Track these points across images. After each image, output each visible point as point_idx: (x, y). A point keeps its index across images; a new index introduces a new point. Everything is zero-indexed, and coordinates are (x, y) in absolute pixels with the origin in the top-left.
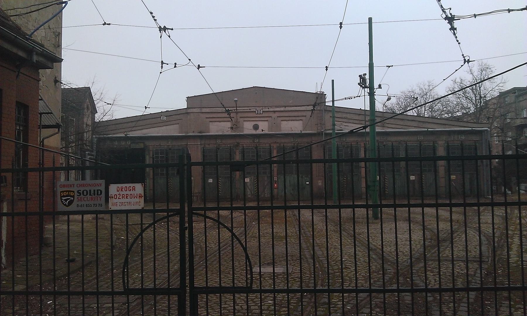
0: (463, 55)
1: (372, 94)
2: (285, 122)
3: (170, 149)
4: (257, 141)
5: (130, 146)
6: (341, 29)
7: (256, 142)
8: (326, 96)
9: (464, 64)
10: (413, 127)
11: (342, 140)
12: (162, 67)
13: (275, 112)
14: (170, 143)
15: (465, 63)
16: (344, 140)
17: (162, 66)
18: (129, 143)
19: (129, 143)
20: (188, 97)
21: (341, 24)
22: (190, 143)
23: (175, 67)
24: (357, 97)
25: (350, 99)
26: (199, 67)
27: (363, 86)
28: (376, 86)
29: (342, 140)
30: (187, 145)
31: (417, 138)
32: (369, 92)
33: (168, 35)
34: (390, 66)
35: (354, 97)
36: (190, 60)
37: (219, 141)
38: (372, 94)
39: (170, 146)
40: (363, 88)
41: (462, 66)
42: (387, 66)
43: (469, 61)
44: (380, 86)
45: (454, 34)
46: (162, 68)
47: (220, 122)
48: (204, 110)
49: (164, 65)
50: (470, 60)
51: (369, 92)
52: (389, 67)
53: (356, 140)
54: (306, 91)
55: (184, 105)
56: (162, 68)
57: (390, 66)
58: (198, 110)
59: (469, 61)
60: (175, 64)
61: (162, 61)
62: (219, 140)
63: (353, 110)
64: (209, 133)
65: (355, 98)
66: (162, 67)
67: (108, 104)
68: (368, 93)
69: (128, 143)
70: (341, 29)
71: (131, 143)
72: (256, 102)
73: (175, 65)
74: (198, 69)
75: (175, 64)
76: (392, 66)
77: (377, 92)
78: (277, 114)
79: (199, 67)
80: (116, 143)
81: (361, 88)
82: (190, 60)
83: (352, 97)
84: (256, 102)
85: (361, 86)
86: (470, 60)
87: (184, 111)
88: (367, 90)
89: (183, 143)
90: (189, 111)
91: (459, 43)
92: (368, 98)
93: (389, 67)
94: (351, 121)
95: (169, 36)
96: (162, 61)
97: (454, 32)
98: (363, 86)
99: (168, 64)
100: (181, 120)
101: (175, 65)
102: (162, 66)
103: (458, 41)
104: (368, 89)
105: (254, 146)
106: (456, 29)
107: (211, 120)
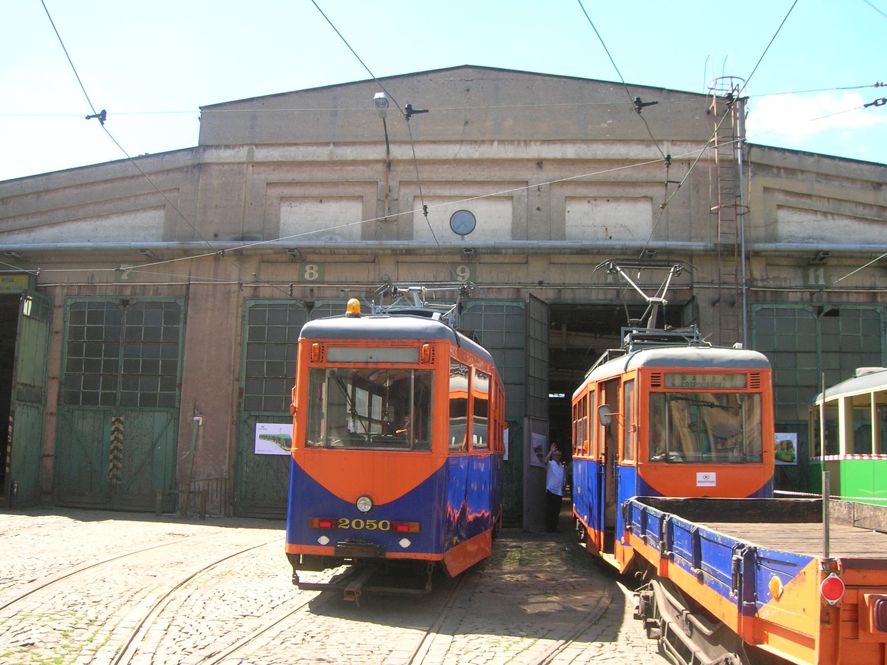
2: (583, 207)
3: (125, 303)
11: (812, 282)
13: (540, 163)
16: (821, 282)
29: (812, 282)
39: (128, 292)
54: (668, 87)
58: (242, 154)
62: (311, 268)
63: (854, 166)
72: (466, 123)
84: (466, 123)
87: (188, 160)
90: (211, 156)
94: (847, 209)
107: (287, 191)
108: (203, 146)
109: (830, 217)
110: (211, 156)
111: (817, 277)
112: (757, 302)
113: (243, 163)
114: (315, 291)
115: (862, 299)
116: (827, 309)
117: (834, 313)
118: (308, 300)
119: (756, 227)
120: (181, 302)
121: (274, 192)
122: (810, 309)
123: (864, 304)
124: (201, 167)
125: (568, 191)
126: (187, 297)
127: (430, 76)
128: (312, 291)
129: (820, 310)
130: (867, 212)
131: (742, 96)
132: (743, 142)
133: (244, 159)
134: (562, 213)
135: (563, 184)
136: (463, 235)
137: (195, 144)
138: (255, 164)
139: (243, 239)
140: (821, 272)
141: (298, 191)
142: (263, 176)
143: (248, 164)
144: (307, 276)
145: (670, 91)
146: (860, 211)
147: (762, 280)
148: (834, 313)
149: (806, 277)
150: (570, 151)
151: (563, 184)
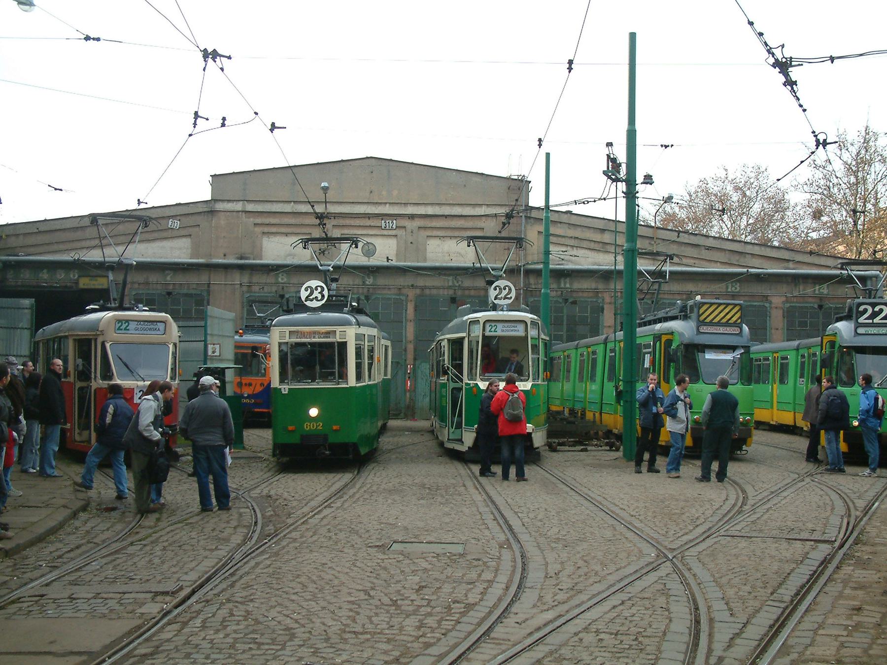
0: (813, 132)
1: (631, 196)
3: (169, 294)
4: (369, 281)
5: (77, 283)
6: (570, 72)
7: (367, 283)
8: (530, 185)
9: (817, 148)
10: (719, 264)
11: (562, 285)
12: (195, 124)
13: (412, 217)
14: (168, 278)
15: (817, 146)
16: (568, 286)
17: (195, 121)
18: (74, 276)
19: (74, 276)
20: (215, 175)
21: (571, 62)
22: (218, 279)
23: (223, 125)
24: (600, 199)
25: (584, 203)
26: (273, 127)
27: (613, 177)
28: (639, 178)
29: (562, 285)
30: (209, 285)
31: (727, 288)
32: (625, 191)
33: (221, 66)
34: (668, 146)
35: (593, 200)
36: (256, 113)
37: (282, 279)
38: (631, 196)
39: (171, 287)
40: (614, 181)
41: (813, 153)
42: (662, 146)
43: (825, 144)
44: (648, 180)
45: (793, 91)
46: (195, 127)
47: (287, 234)
48: (250, 207)
49: (199, 120)
50: (828, 141)
51: (625, 191)
52: (666, 147)
53: (593, 286)
55: (205, 193)
56: (195, 127)
57: (668, 146)
58: (238, 206)
59: (825, 144)
60: (224, 119)
61: (196, 113)
63: (590, 220)
64: (261, 260)
65: (595, 201)
66: (195, 124)
67: (56, 189)
68: (623, 192)
69: (72, 276)
70: (570, 72)
71: (79, 276)
73: (224, 122)
74: (272, 130)
75: (224, 119)
76: (672, 146)
77: (642, 190)
78: (418, 223)
79: (273, 127)
80: (45, 275)
81: (609, 181)
82: (256, 113)
83: (589, 200)
85: (609, 177)
86: (828, 141)
88: (622, 186)
89: (204, 278)
90: (220, 206)
91: (804, 110)
92: (622, 203)
93: (666, 147)
95: (222, 69)
96: (196, 113)
97: (792, 88)
98: (613, 177)
99: (207, 119)
100: (197, 229)
101: (224, 122)
102: (195, 121)
103: (801, 106)
104: (624, 183)
105: (363, 294)
106: (795, 83)
107: (266, 230)
108: (214, 200)
109: (575, 249)
110: (220, 206)
111: (566, 284)
112: (532, 296)
113: (238, 212)
114: (285, 288)
115: (591, 294)
116: (570, 301)
117: (574, 303)
118: (281, 293)
119: (533, 254)
120: (205, 294)
121: (258, 230)
122: (561, 301)
123: (591, 297)
124: (212, 212)
125: (429, 233)
126: (209, 292)
127: (350, 163)
128: (283, 288)
129: (566, 300)
130: (597, 246)
131: (528, 180)
132: (527, 205)
133: (240, 209)
134: (425, 245)
135: (425, 228)
136: (369, 257)
137: (209, 198)
138: (246, 212)
139: (241, 258)
140: (568, 280)
141: (274, 230)
142: (252, 219)
143: (242, 211)
144: (280, 280)
145: (487, 175)
146: (592, 245)
147: (535, 284)
148: (574, 303)
149: (559, 283)
150: (430, 211)
151: (425, 228)
